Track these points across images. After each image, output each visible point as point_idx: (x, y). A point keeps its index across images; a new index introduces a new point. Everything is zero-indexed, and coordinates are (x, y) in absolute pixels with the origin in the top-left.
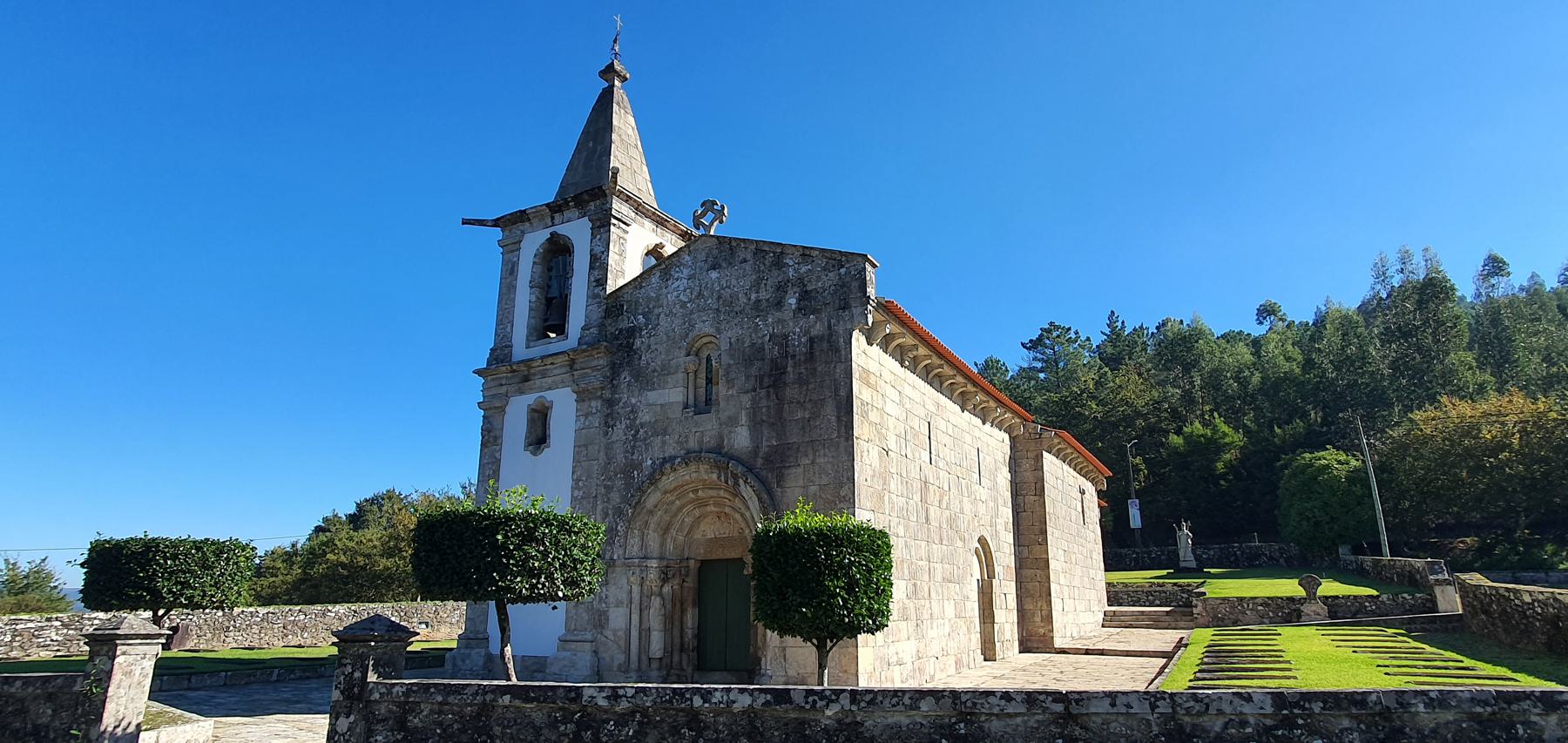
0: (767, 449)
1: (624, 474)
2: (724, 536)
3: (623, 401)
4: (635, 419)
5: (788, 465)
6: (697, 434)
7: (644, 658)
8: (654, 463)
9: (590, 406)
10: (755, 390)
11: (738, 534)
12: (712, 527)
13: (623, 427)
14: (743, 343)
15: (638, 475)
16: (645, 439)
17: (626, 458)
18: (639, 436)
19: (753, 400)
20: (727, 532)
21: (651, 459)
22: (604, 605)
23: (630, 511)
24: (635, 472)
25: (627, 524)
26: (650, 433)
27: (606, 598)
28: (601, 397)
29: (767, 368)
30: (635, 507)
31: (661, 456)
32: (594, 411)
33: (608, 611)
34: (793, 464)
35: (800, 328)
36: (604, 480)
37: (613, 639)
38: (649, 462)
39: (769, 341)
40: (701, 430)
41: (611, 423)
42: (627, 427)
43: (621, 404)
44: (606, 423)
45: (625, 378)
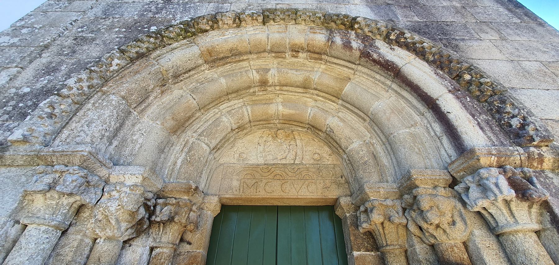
2: (284, 162)
20: (291, 156)
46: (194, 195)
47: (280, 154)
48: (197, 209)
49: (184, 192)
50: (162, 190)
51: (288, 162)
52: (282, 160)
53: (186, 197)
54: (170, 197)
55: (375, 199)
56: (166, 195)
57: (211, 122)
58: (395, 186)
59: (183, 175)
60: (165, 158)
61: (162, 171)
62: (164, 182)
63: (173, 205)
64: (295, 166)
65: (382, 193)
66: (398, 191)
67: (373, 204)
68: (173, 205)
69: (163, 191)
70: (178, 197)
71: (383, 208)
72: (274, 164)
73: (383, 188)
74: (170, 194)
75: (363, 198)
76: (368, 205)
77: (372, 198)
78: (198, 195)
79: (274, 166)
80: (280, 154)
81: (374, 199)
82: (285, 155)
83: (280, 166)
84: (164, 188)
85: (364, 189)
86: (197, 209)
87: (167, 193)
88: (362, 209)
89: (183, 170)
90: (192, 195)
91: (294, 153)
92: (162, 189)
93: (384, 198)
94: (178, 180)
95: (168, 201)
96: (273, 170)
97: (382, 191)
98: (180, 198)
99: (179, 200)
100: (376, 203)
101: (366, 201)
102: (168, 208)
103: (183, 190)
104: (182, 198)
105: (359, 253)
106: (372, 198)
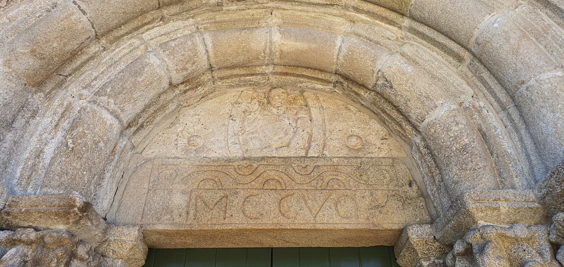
2: (284, 153)
11: (344, 153)
12: (235, 126)
46: (82, 222)
47: (276, 138)
48: (88, 253)
49: (57, 214)
50: (5, 212)
51: (292, 154)
52: (280, 150)
53: (61, 227)
54: (25, 227)
55: (489, 224)
56: (16, 222)
57: (122, 66)
58: (532, 195)
59: (57, 177)
60: (15, 142)
61: (9, 170)
62: (12, 192)
63: (29, 243)
64: (307, 162)
65: (503, 210)
66: (540, 206)
67: (485, 235)
68: (29, 243)
69: (8, 214)
70: (42, 226)
71: (507, 244)
72: (263, 158)
73: (506, 200)
74: (24, 220)
75: (460, 225)
76: (473, 238)
77: (481, 223)
78: (92, 223)
79: (263, 162)
80: (276, 138)
81: (486, 224)
82: (286, 139)
83: (276, 161)
84: (9, 206)
85: (463, 204)
86: (88, 253)
87: (16, 218)
88: (459, 247)
89: (57, 168)
90: (77, 222)
91: (306, 136)
92: (4, 208)
93: (508, 223)
94: (45, 190)
95: (19, 236)
96: (261, 169)
97: (504, 207)
98: (48, 229)
99: (45, 232)
100: (492, 234)
101: (468, 229)
102: (18, 251)
103: (54, 210)
104: (52, 227)
106: (481, 223)
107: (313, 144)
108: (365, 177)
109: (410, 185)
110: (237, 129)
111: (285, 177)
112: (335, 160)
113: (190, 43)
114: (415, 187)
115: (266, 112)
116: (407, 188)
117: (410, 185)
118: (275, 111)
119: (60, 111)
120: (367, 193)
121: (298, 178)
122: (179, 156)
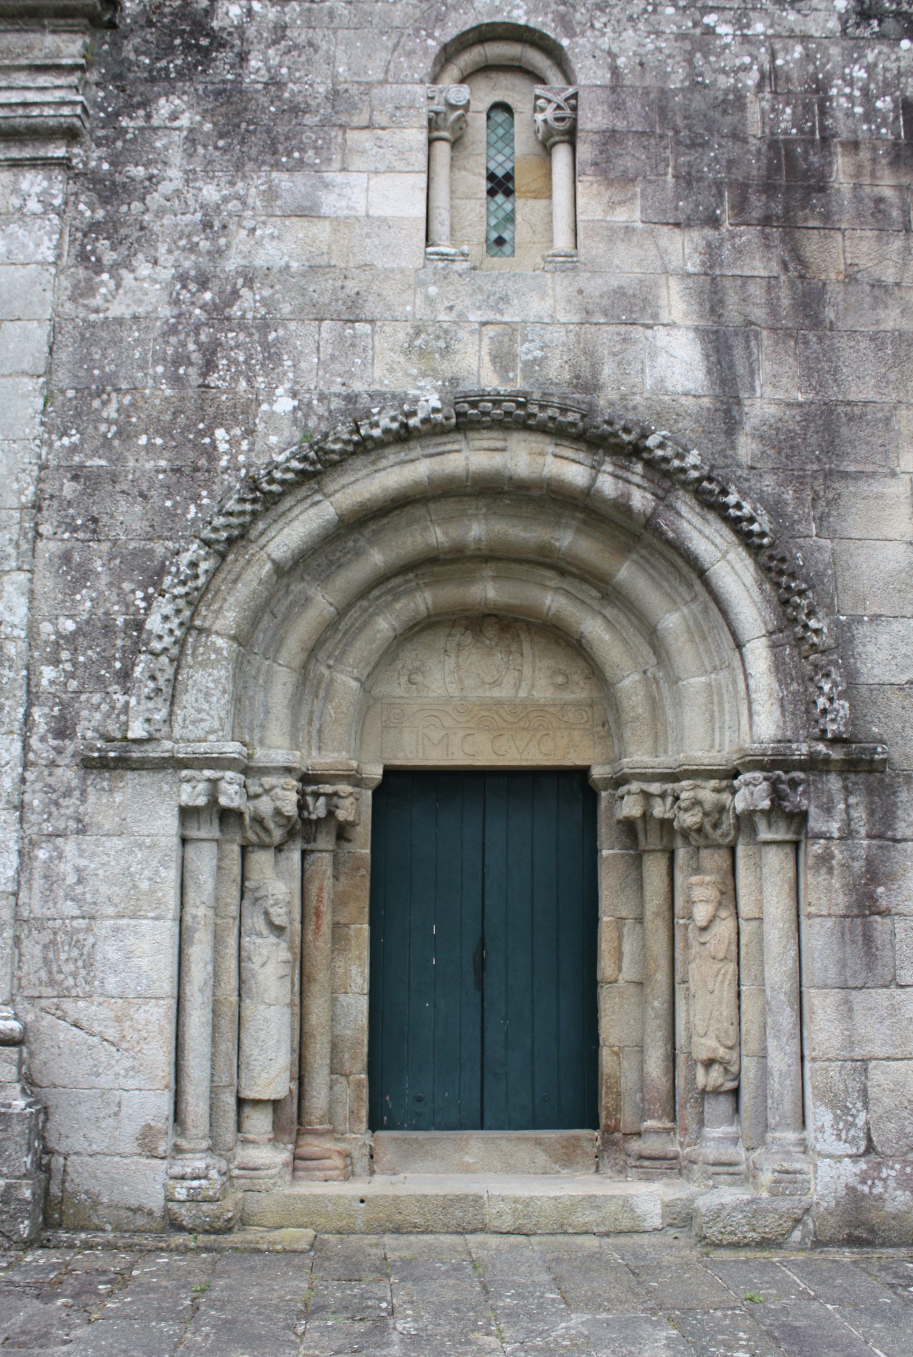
0: (772, 410)
1: (165, 432)
3: (166, 187)
4: (218, 253)
5: (852, 468)
6: (490, 331)
7: (232, 1101)
8: (304, 408)
9: (16, 191)
10: (714, 222)
13: (167, 274)
14: (666, 76)
15: (233, 443)
16: (264, 326)
17: (177, 381)
18: (235, 311)
19: (711, 253)
21: (294, 395)
22: (70, 908)
23: (204, 566)
24: (220, 433)
25: (187, 613)
26: (286, 309)
27: (80, 882)
28: (64, 164)
29: (754, 167)
30: (223, 556)
31: (337, 388)
32: (33, 205)
33: (89, 930)
34: (869, 468)
35: (870, 68)
36: (74, 449)
37: (111, 1034)
38: (284, 404)
39: (760, 87)
40: (507, 318)
41: (109, 257)
42: (183, 279)
43: (155, 199)
44: (83, 257)
45: (174, 117)
105: (611, 851)
107: (523, 684)
108: (565, 719)
109: (603, 725)
110: (452, 665)
111: (496, 717)
112: (542, 701)
113: (412, 604)
114: (607, 727)
115: (479, 645)
116: (600, 728)
117: (603, 725)
118: (487, 642)
119: (315, 682)
120: (566, 733)
121: (508, 718)
122: (403, 694)
